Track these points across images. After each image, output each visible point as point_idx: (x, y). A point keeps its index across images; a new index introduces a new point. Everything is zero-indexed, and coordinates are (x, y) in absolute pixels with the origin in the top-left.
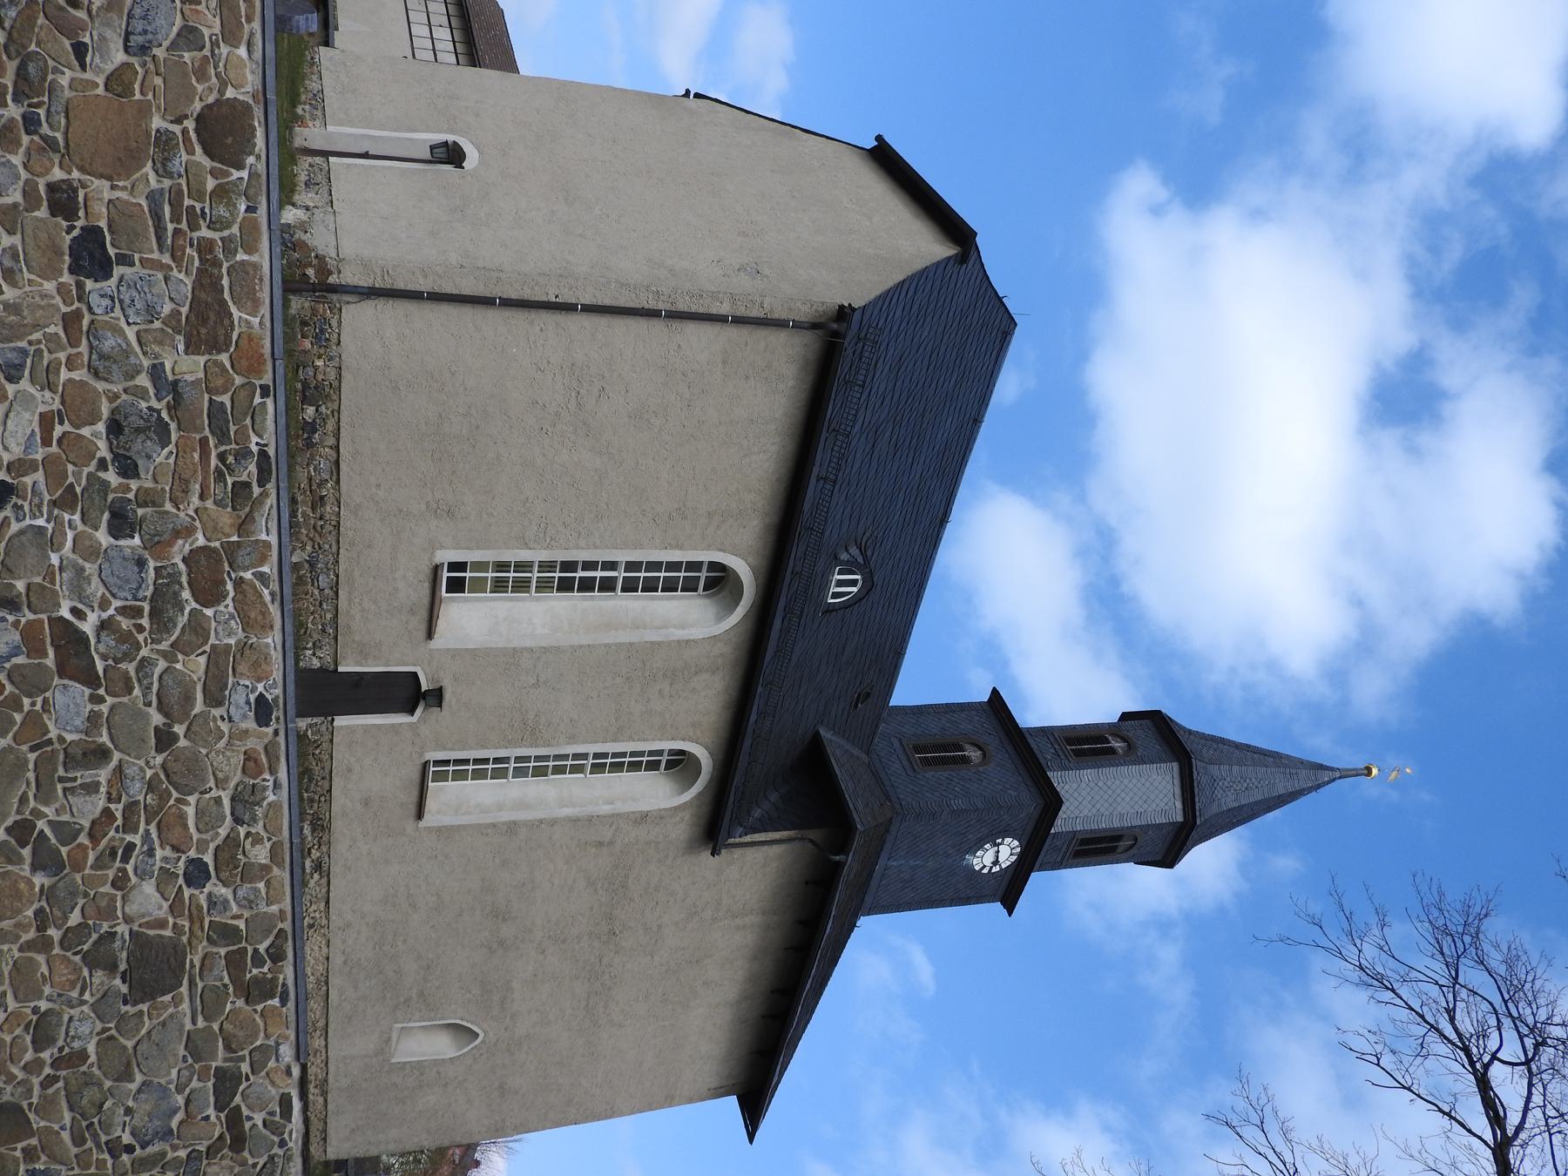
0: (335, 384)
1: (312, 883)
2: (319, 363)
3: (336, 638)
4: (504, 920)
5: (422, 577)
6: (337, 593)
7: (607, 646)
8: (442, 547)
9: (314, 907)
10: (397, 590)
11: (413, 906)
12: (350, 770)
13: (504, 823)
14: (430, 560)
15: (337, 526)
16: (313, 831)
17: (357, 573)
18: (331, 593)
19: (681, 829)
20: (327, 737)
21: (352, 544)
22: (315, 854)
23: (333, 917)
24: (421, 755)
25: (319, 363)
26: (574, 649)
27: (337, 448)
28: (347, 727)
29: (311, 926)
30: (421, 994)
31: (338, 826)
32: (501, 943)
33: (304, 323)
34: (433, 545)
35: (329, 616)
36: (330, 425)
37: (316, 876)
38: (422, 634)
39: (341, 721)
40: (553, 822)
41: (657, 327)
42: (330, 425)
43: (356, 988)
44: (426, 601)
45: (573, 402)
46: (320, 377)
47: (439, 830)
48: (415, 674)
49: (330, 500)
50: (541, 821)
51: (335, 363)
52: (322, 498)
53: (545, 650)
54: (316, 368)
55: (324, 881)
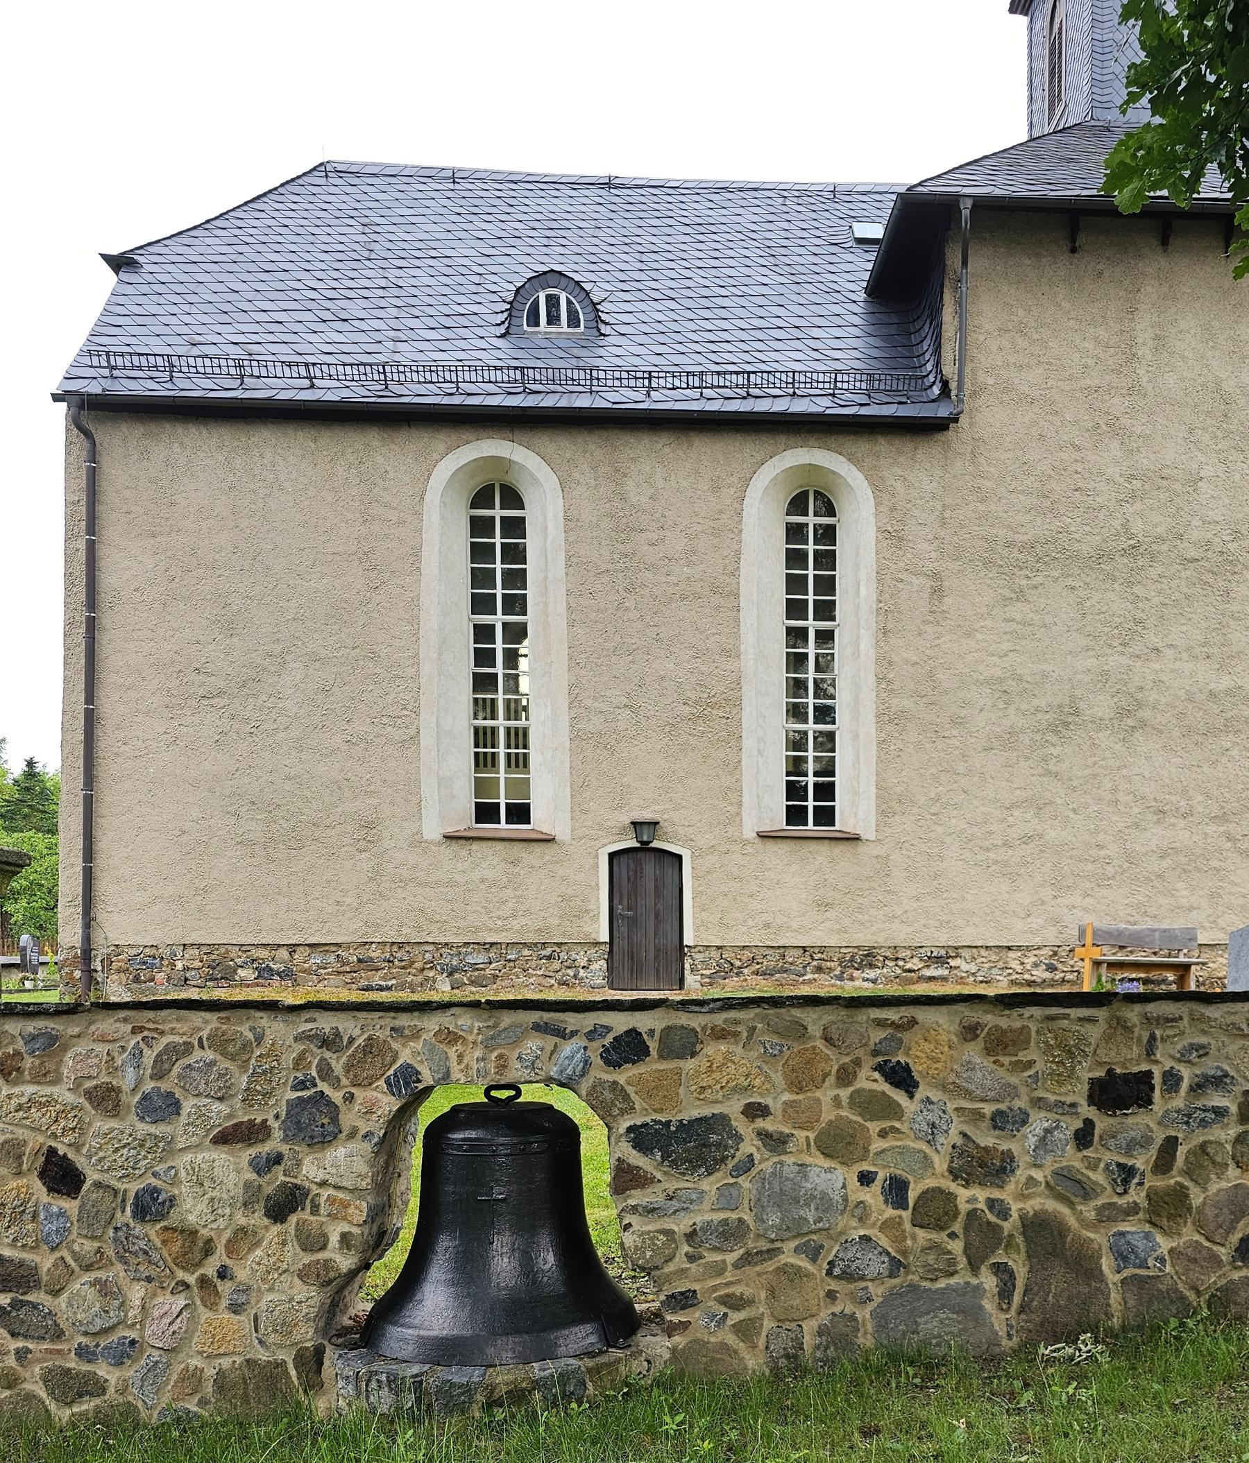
0: (204, 949)
1: (965, 967)
2: (179, 965)
3: (560, 944)
4: (1076, 713)
5: (464, 853)
6: (492, 944)
7: (572, 624)
8: (419, 832)
9: (1015, 965)
10: (482, 881)
11: (1027, 839)
12: (767, 926)
13: (879, 729)
14: (440, 844)
15: (401, 946)
16: (871, 966)
17: (461, 923)
18: (494, 950)
19: (917, 472)
20: (715, 954)
21: (419, 928)
22: (915, 964)
23: (1038, 941)
24: (746, 843)
25: (179, 965)
26: (574, 664)
27: (292, 948)
28: (696, 929)
29: (1051, 968)
30: (1222, 819)
31: (863, 937)
32: (1123, 713)
33: (137, 979)
34: (417, 842)
35: (526, 952)
36: (263, 953)
37: (953, 963)
38: (549, 850)
39: (688, 940)
40: (885, 662)
41: (106, 619)
42: (263, 953)
43: (1191, 909)
44: (499, 846)
45: (212, 702)
46: (197, 964)
47: (884, 813)
48: (612, 856)
49: (362, 953)
50: (880, 679)
51: (179, 951)
52: (359, 961)
53: (574, 701)
54: (186, 969)
55: (965, 953)
